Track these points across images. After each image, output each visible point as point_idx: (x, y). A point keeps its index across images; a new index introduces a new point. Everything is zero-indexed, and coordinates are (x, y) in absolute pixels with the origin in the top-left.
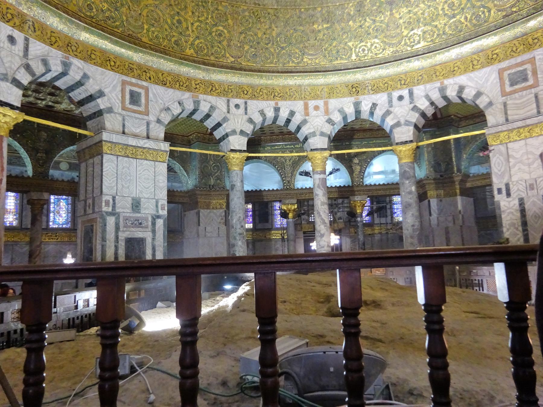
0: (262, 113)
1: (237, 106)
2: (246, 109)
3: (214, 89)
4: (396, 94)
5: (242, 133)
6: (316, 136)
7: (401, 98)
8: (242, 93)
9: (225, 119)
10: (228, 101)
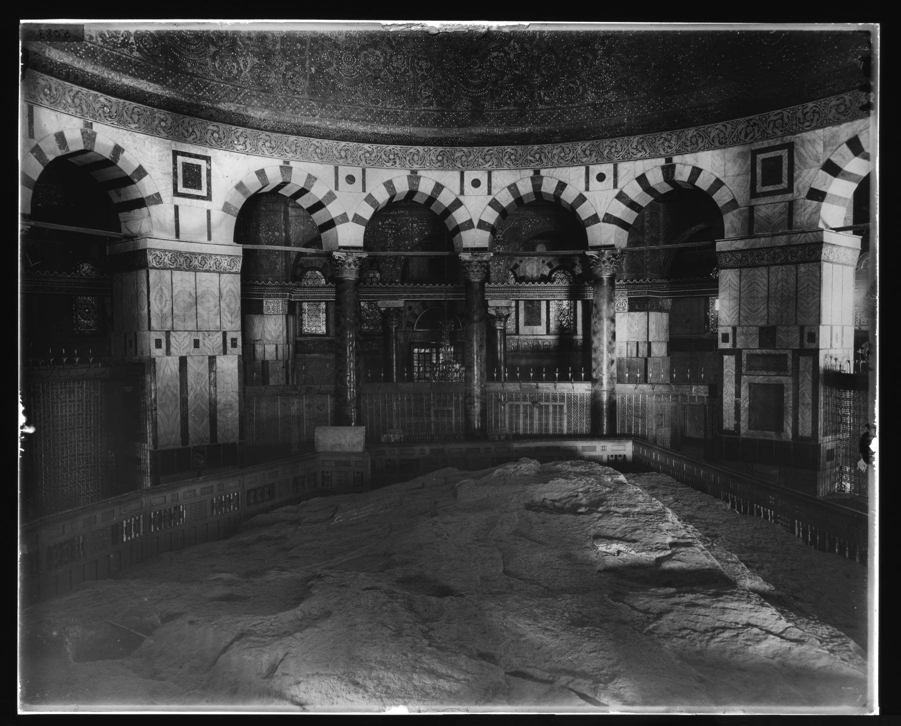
0: (389, 185)
5: (357, 219)
9: (331, 197)
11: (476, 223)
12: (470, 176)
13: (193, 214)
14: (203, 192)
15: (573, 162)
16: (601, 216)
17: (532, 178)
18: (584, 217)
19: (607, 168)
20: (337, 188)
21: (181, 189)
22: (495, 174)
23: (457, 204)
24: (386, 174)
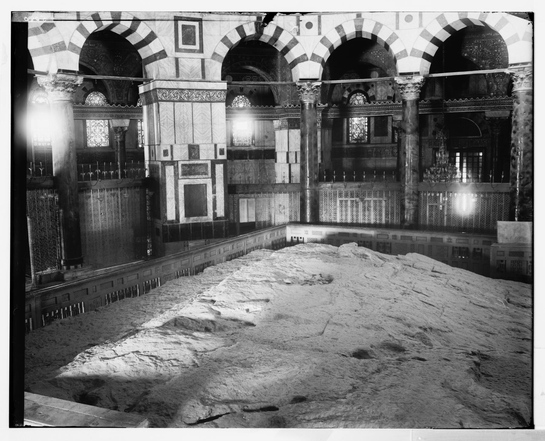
0: (339, 29)
1: (309, 25)
2: (319, 28)
6: (407, 56)
11: (409, 52)
13: (190, 62)
16: (309, 56)
18: (436, 48)
23: (394, 37)
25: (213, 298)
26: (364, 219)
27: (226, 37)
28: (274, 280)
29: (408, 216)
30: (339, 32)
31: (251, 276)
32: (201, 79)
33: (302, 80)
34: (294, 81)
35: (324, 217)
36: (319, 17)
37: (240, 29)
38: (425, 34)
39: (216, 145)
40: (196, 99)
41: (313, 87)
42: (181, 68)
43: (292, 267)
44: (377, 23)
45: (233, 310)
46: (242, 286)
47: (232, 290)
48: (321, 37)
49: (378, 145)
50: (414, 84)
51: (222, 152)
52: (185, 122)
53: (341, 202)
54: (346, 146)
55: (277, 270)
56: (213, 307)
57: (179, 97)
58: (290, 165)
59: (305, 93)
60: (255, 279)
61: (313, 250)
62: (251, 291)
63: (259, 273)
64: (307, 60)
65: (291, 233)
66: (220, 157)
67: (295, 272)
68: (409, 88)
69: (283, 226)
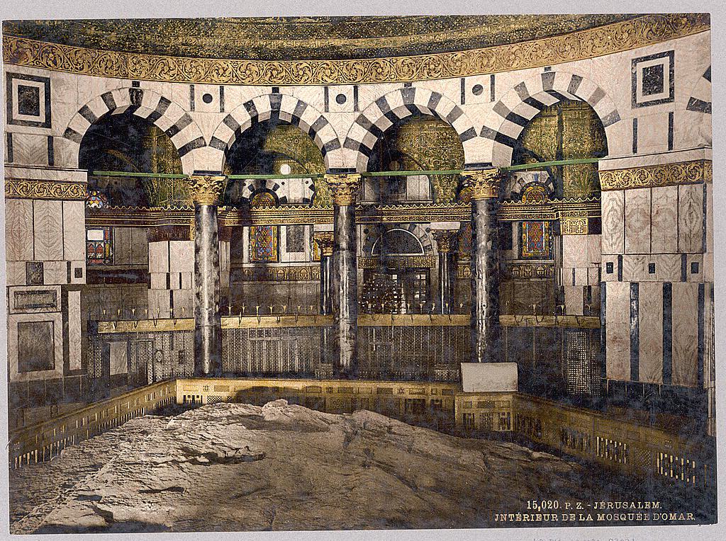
0: (249, 105)
1: (207, 98)
2: (222, 102)
3: (166, 69)
4: (471, 82)
7: (477, 89)
8: (214, 73)
10: (192, 90)
12: (334, 92)
14: (42, 118)
15: (448, 74)
17: (403, 91)
19: (484, 80)
20: (192, 108)
21: (16, 115)
22: (361, 88)
23: (322, 121)
24: (247, 93)
25: (97, 492)
26: (285, 366)
27: (85, 107)
28: (183, 459)
29: (346, 358)
30: (248, 110)
31: (147, 455)
32: (47, 165)
33: (197, 173)
34: (185, 172)
35: (228, 365)
36: (222, 89)
37: (107, 97)
38: (362, 121)
39: (69, 264)
40: (39, 194)
41: (212, 184)
42: (15, 148)
43: (203, 439)
44: (299, 102)
45: (131, 509)
46: (137, 471)
47: (124, 478)
48: (225, 115)
49: (291, 264)
50: (350, 184)
51: (78, 273)
52: (22, 228)
53: (253, 343)
54: (247, 266)
55: (184, 445)
56: (99, 506)
57: (11, 191)
58: (172, 292)
59: (202, 190)
60: (155, 459)
61: (229, 414)
62: (153, 477)
63: (160, 451)
64: (205, 145)
65: (183, 390)
66: (75, 281)
67: (211, 446)
68: (343, 189)
69: (170, 379)
